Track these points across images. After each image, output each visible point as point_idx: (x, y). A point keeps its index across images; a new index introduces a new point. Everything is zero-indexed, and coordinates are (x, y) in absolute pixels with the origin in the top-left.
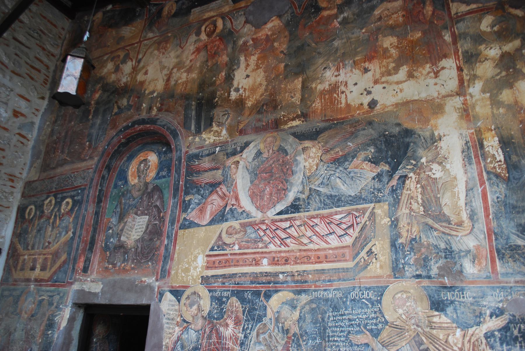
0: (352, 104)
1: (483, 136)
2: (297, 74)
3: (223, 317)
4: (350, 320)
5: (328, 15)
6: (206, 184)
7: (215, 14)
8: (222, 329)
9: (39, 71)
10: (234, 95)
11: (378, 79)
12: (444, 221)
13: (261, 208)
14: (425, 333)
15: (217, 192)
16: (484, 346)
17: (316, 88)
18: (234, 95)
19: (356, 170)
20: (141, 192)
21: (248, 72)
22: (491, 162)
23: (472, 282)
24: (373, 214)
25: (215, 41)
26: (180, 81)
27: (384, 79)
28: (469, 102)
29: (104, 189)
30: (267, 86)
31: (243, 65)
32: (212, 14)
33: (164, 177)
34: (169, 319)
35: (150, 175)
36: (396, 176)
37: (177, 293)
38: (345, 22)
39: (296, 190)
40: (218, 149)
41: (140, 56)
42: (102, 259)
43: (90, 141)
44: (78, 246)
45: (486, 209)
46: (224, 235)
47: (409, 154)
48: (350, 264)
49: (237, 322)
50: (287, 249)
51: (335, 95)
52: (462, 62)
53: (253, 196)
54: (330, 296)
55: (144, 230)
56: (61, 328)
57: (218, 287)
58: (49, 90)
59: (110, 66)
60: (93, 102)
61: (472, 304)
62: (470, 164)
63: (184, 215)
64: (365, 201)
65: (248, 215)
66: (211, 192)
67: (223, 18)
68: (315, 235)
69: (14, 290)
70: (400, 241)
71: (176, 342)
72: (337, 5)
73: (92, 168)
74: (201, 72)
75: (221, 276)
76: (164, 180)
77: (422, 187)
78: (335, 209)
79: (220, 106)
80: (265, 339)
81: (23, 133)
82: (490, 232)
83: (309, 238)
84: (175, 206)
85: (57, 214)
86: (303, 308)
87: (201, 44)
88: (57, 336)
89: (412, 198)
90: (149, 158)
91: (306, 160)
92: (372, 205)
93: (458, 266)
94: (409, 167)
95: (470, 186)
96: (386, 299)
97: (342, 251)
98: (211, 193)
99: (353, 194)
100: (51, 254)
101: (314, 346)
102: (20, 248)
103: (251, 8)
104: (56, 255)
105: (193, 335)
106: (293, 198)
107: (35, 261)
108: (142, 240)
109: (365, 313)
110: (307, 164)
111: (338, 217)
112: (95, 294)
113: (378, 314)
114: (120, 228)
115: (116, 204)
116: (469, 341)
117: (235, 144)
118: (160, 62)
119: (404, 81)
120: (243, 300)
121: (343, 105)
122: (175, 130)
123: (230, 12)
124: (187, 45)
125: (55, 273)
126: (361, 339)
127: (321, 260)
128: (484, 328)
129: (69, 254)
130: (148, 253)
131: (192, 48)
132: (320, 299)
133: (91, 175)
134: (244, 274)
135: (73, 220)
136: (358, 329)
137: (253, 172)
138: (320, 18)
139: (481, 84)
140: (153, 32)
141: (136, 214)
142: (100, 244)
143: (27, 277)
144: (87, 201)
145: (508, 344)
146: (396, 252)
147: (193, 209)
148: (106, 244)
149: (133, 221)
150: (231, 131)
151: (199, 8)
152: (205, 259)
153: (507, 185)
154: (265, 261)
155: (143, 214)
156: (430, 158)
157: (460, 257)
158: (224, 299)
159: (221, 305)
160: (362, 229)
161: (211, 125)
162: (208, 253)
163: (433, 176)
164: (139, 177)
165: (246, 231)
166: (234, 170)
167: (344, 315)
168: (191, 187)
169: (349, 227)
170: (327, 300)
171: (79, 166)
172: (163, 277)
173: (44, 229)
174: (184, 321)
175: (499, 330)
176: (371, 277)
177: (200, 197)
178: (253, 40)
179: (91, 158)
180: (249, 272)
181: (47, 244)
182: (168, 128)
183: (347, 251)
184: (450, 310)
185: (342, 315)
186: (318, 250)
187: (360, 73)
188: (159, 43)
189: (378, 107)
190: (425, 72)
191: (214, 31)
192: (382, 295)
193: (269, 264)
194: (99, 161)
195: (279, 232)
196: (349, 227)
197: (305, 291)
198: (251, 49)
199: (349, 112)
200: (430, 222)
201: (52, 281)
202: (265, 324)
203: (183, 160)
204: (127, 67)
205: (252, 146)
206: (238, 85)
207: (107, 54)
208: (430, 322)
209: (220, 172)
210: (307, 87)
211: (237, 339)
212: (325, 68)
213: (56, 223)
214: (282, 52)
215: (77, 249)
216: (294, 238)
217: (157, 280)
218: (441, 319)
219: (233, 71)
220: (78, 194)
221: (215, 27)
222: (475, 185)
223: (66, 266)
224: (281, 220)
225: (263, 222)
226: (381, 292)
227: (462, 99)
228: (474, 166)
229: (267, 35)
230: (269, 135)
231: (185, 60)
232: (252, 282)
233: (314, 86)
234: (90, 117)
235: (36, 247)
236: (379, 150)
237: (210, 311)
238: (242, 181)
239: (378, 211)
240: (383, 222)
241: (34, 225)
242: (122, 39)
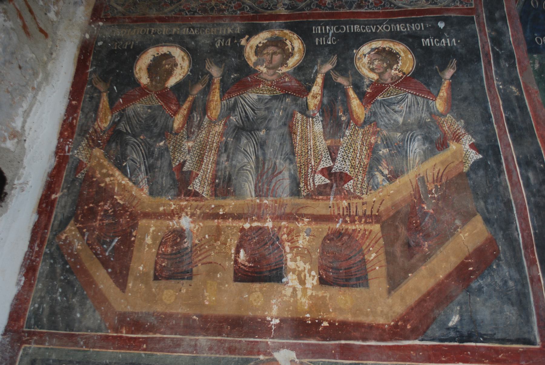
85: (340, 80)
100: (375, 218)
102: (129, 187)
125: (439, 296)
181: (320, 180)
201: (435, 330)
213: (348, 110)
220: (439, 34)
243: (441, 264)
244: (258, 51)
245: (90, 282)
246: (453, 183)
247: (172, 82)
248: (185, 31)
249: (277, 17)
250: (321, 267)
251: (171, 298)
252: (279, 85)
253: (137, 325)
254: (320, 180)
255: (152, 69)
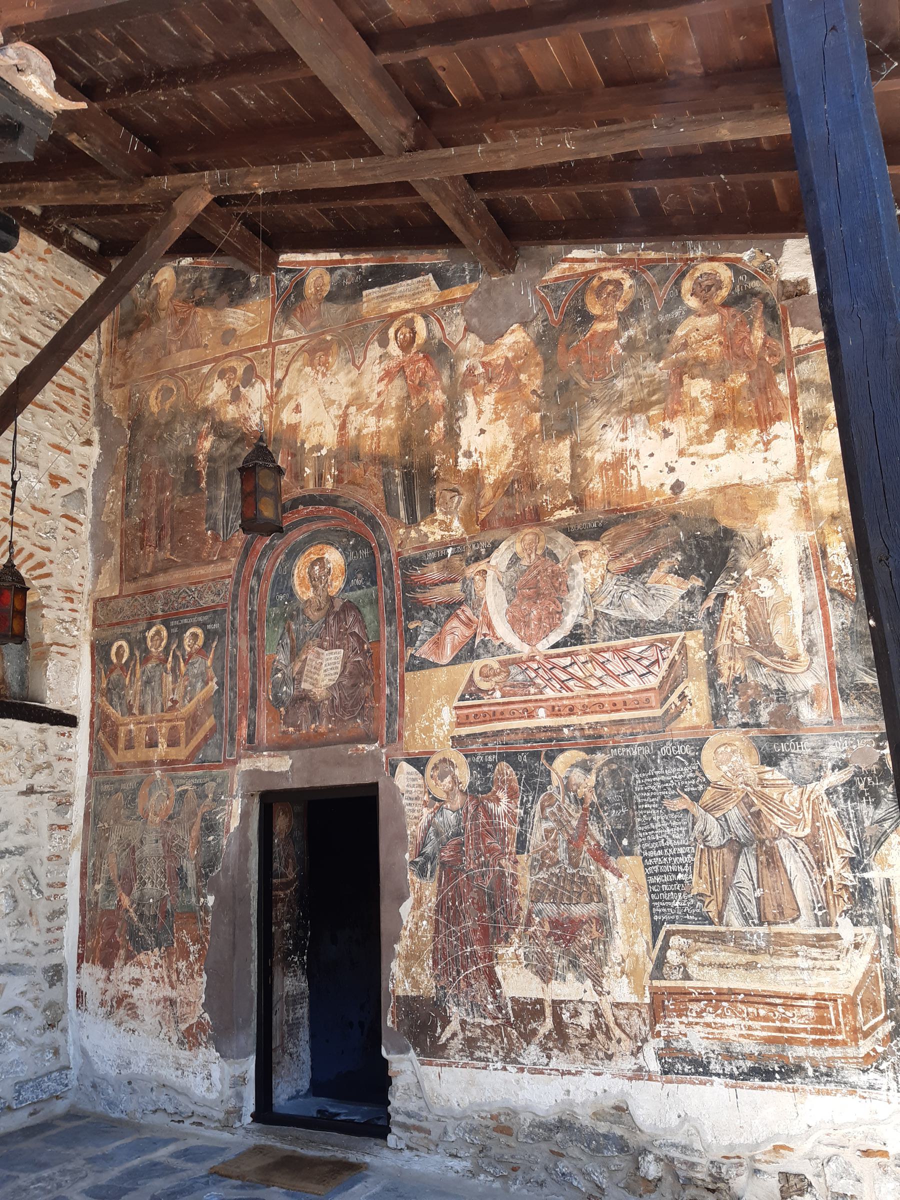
0: (648, 485)
1: (827, 541)
2: (561, 435)
3: (490, 790)
4: (662, 782)
5: (604, 331)
6: (439, 603)
7: (409, 306)
8: (491, 805)
9: (72, 391)
10: (464, 464)
11: (683, 449)
12: (776, 655)
13: (527, 639)
14: (755, 792)
15: (458, 616)
16: (825, 804)
17: (592, 458)
18: (464, 464)
19: (657, 586)
20: (323, 612)
21: (482, 424)
22: (836, 577)
23: (811, 730)
24: (683, 646)
25: (418, 361)
26: (365, 432)
27: (692, 449)
28: (809, 490)
29: (256, 608)
30: (516, 449)
31: (472, 410)
32: (403, 305)
33: (360, 587)
34: (411, 799)
35: (334, 584)
36: (713, 595)
37: (419, 763)
38: (631, 346)
39: (576, 614)
40: (450, 551)
41: (279, 375)
42: (273, 719)
43: (213, 528)
44: (233, 703)
45: (828, 637)
46: (477, 677)
47: (728, 565)
48: (658, 712)
49: (512, 795)
50: (570, 694)
51: (622, 472)
52: (802, 428)
53: (515, 623)
54: (635, 753)
55: (339, 671)
56: (232, 830)
57: (478, 750)
58: (95, 425)
59: (218, 390)
60: (201, 457)
61: (810, 756)
62: (809, 579)
63: (410, 651)
64: (672, 628)
65: (510, 649)
66: (449, 616)
67: (425, 317)
68: (608, 674)
69: (122, 781)
70: (720, 681)
71: (427, 829)
72: (618, 313)
73: (230, 577)
74: (400, 417)
75: (481, 734)
76: (359, 592)
77: (748, 610)
78: (632, 640)
79: (443, 480)
80: (553, 814)
81: (73, 513)
82: (832, 668)
83: (600, 679)
84: (392, 637)
85: (178, 653)
86: (599, 770)
87: (393, 364)
88: (226, 842)
89: (734, 624)
90: (326, 556)
91: (586, 571)
92: (682, 634)
93: (793, 711)
94: (729, 582)
95: (808, 608)
96: (707, 754)
97: (645, 695)
98: (449, 617)
99: (655, 619)
100: (182, 719)
101: (619, 817)
102: (114, 713)
103: (472, 302)
104: (194, 721)
105: (451, 817)
106: (572, 625)
107: (152, 732)
108: (339, 685)
109: (681, 773)
110: (588, 576)
111: (637, 650)
112: (281, 774)
113: (697, 773)
114: (296, 669)
115: (280, 631)
116: (808, 799)
117: (476, 543)
118: (322, 391)
119: (722, 455)
120: (516, 766)
121: (635, 488)
122: (373, 517)
123: (435, 305)
124: (366, 362)
125: (198, 748)
126: (678, 804)
127: (618, 707)
128: (825, 783)
129: (219, 717)
130: (352, 706)
131: (377, 370)
132: (622, 757)
133: (231, 588)
134: (514, 731)
135: (213, 662)
136: (673, 792)
137: (510, 587)
138: (592, 335)
139: (828, 463)
140: (293, 327)
141: (321, 646)
142: (265, 696)
143: (144, 759)
144: (234, 631)
145: (853, 801)
146: (716, 696)
147: (423, 642)
148: (275, 696)
149: (318, 658)
150: (467, 523)
151: (376, 289)
152: (454, 712)
153: (855, 608)
154: (542, 712)
155: (333, 646)
156: (757, 570)
157: (795, 699)
158: (490, 766)
159: (485, 774)
160: (671, 666)
161: (433, 511)
162: (456, 703)
163: (761, 595)
164: (315, 587)
165: (509, 672)
166: (481, 584)
167: (655, 776)
168: (415, 608)
169: (653, 663)
170: (631, 759)
171: (202, 572)
172: (390, 741)
173: (157, 679)
174: (435, 799)
175: (843, 785)
176: (685, 729)
177: (432, 624)
178: (484, 364)
179: (223, 559)
180: (520, 727)
181: (170, 704)
182: (361, 514)
183: (651, 695)
184: (784, 764)
185: (652, 777)
186: (614, 694)
187: (658, 438)
188: (312, 352)
189: (685, 493)
190: (750, 442)
191: (413, 340)
192: (701, 749)
193: (548, 716)
194: (241, 564)
195: (555, 671)
196: (653, 663)
197: (600, 749)
198: (482, 382)
199: (643, 499)
200: (758, 656)
202: (551, 794)
203: (394, 567)
204: (257, 394)
205: (503, 546)
206: (469, 446)
207: (206, 362)
208: (761, 779)
209: (458, 586)
210: (579, 456)
211: (514, 816)
212: (605, 426)
214: (534, 392)
215: (233, 709)
216: (579, 679)
217: (382, 746)
218: (773, 774)
219: (458, 420)
221: (414, 332)
222: (815, 607)
223: (218, 736)
224: (558, 656)
225: (532, 659)
226: (699, 745)
227: (800, 485)
228: (814, 582)
229: (507, 358)
230: (526, 531)
231: (367, 391)
232: (526, 741)
233: (589, 454)
234: (203, 485)
235: (149, 710)
236: (690, 559)
237: (471, 783)
238: (494, 599)
239: (690, 643)
240: (697, 657)
241: (134, 673)
242: (229, 335)
243: (200, 735)
244: (152, 638)
245: (108, 753)
246: (207, 701)
247: (124, 661)
248: (126, 630)
249: (157, 617)
250: (168, 741)
251: (129, 756)
252: (158, 658)
253: (121, 767)
254: (170, 704)
255: (117, 654)
